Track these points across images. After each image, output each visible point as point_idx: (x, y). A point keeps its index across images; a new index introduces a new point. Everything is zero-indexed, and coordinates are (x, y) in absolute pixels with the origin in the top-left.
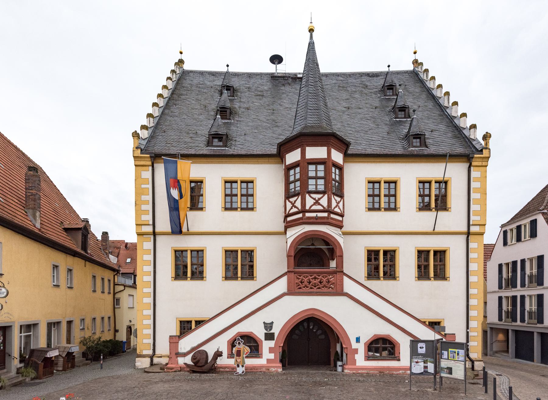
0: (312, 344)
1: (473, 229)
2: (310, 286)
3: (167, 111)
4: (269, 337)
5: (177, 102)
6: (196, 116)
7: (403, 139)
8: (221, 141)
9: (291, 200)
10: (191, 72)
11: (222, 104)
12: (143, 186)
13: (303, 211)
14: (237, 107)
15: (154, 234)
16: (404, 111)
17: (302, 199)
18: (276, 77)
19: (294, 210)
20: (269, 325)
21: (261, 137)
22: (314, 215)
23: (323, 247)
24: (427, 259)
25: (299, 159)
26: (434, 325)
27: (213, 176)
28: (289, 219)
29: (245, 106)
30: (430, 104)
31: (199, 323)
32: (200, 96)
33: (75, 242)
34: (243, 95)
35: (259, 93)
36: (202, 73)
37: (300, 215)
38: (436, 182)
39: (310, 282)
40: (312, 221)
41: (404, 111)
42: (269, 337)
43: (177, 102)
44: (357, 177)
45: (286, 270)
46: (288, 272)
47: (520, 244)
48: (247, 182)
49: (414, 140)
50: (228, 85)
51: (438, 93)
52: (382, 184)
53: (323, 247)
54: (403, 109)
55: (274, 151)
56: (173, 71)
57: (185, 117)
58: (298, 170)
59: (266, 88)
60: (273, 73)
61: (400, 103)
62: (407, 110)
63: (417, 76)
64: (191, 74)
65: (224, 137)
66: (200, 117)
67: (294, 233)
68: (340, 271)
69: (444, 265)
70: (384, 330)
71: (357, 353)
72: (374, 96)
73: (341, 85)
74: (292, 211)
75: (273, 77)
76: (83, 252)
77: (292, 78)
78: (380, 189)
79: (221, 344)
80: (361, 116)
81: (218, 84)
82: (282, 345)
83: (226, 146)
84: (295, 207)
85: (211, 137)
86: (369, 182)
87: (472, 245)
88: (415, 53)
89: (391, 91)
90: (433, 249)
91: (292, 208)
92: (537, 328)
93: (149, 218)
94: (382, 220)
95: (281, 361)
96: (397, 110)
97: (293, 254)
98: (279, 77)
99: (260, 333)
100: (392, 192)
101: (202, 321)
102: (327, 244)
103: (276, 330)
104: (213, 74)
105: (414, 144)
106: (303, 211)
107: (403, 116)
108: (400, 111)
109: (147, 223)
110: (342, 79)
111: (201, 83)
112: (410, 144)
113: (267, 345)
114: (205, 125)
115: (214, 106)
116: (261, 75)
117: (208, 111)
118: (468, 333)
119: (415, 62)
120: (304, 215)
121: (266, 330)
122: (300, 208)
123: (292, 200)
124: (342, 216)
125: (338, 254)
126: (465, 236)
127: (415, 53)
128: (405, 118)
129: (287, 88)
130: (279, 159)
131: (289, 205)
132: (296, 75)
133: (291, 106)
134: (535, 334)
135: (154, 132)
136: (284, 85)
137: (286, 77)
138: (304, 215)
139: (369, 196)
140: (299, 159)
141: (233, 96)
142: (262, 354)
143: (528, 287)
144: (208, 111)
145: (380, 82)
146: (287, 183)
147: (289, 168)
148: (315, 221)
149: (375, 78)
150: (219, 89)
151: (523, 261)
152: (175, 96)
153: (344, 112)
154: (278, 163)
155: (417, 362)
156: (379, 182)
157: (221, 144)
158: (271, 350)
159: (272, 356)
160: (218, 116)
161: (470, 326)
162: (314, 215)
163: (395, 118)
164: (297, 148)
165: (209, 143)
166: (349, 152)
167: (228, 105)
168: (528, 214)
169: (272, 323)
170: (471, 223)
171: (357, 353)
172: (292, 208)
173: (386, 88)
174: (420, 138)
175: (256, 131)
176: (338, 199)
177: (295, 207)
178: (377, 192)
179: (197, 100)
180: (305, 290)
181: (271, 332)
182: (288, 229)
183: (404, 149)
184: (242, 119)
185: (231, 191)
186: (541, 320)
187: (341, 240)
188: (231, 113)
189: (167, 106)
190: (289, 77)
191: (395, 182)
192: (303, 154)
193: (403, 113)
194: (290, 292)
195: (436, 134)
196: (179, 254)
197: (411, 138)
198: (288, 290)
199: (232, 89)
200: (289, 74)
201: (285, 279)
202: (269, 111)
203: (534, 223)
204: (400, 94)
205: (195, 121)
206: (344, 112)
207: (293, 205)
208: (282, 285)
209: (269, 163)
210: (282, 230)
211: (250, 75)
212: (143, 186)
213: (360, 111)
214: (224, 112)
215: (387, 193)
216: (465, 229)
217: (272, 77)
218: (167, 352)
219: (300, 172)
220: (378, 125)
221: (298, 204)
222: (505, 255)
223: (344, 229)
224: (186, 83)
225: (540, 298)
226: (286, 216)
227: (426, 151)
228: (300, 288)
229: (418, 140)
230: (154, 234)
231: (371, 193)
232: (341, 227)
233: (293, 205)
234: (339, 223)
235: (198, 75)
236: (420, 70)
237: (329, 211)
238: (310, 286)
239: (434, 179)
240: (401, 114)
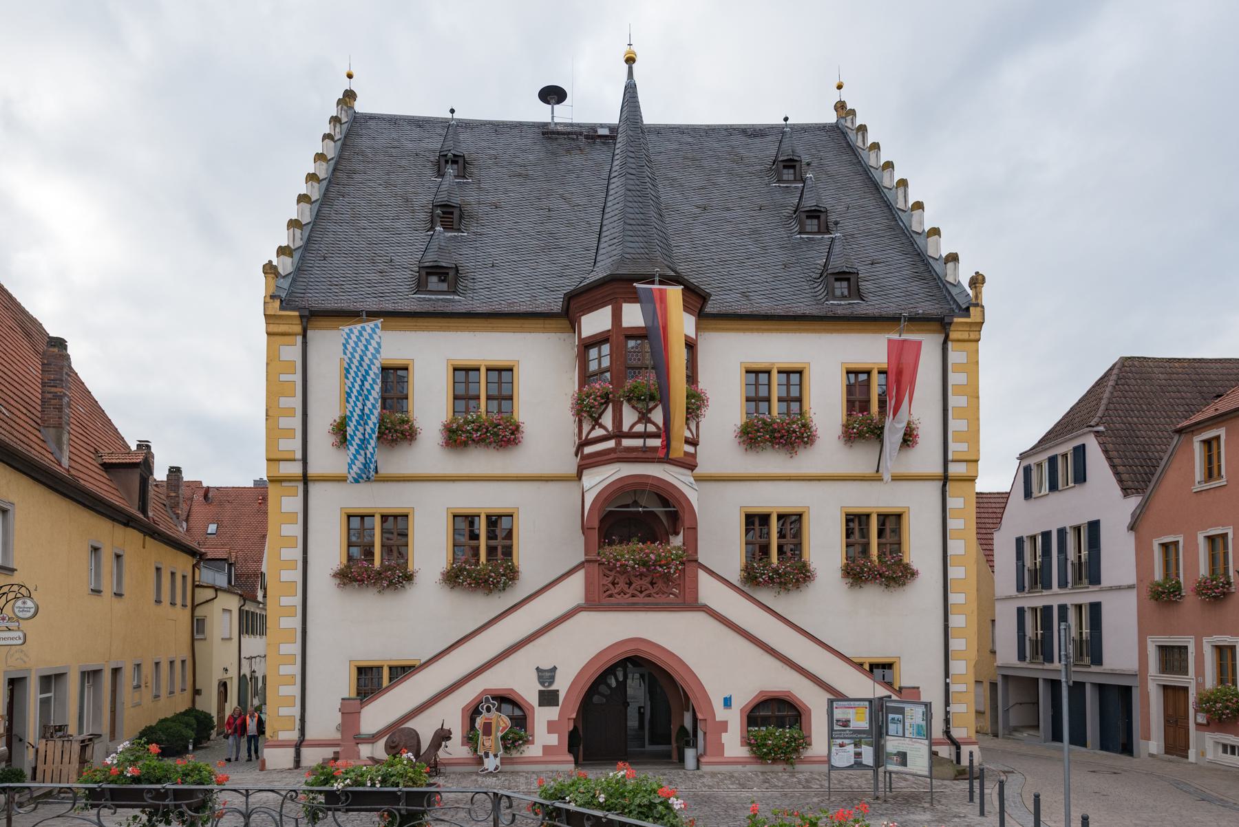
0: (635, 712)
1: (955, 469)
2: (631, 591)
3: (326, 210)
4: (548, 698)
5: (346, 190)
6: (388, 223)
7: (814, 280)
8: (443, 281)
10: (372, 117)
11: (443, 197)
13: (618, 435)
14: (470, 199)
15: (305, 479)
16: (818, 217)
17: (614, 410)
18: (553, 133)
19: (598, 432)
20: (548, 674)
21: (526, 271)
22: (638, 442)
23: (659, 510)
24: (865, 534)
25: (609, 327)
26: (880, 669)
27: (431, 359)
28: (588, 450)
29: (491, 198)
30: (870, 203)
31: (401, 672)
32: (393, 176)
33: (124, 493)
34: (483, 173)
35: (518, 170)
36: (394, 121)
37: (611, 444)
38: (880, 372)
39: (630, 584)
40: (634, 455)
41: (818, 217)
42: (548, 698)
43: (346, 190)
44: (726, 364)
45: (581, 558)
46: (587, 561)
47: (1055, 496)
48: (500, 370)
49: (837, 284)
50: (453, 151)
51: (887, 181)
52: (775, 374)
53: (659, 510)
54: (815, 214)
55: (557, 307)
56: (335, 120)
57: (366, 224)
58: (606, 349)
59: (531, 157)
60: (546, 124)
61: (809, 203)
62: (823, 216)
63: (842, 138)
64: (372, 123)
65: (452, 273)
66: (397, 225)
67: (598, 480)
68: (690, 560)
69: (900, 544)
70: (782, 681)
71: (726, 731)
72: (756, 181)
73: (689, 155)
74: (591, 436)
75: (548, 133)
76: (141, 516)
77: (587, 137)
78: (769, 385)
79: (451, 715)
80: (729, 228)
81: (430, 146)
82: (574, 716)
83: (455, 293)
84: (601, 426)
85: (423, 273)
86: (747, 372)
87: (952, 503)
88: (840, 87)
89: (792, 171)
90: (875, 510)
92: (1090, 675)
93: (295, 445)
95: (572, 748)
96: (804, 216)
97: (596, 524)
98: (559, 133)
99: (529, 692)
100: (794, 392)
101: (410, 667)
102: (665, 502)
103: (562, 685)
104: (420, 123)
105: (838, 292)
106: (618, 435)
107: (815, 229)
108: (808, 217)
109: (291, 457)
110: (690, 140)
111: (396, 144)
112: (831, 294)
113: (543, 717)
114: (411, 244)
115: (424, 199)
116: (519, 126)
117: (413, 211)
118: (947, 685)
119: (840, 106)
120: (618, 444)
121: (542, 683)
122: (610, 429)
124: (694, 443)
125: (687, 525)
126: (940, 484)
127: (840, 87)
128: (819, 232)
129: (577, 159)
130: (565, 323)
132: (593, 128)
133: (584, 200)
134: (1088, 687)
135: (302, 258)
136: (568, 151)
137: (575, 133)
138: (618, 444)
139: (748, 400)
140: (609, 327)
141: (464, 177)
142: (532, 736)
143: (1073, 588)
144: (413, 211)
145: (768, 150)
146: (585, 377)
147: (588, 345)
148: (640, 455)
149: (757, 140)
150: (432, 159)
151: (1062, 532)
152: (338, 174)
153: (695, 218)
154: (562, 331)
155: (841, 746)
156: (769, 372)
157: (444, 286)
158: (552, 727)
159: (553, 740)
160: (439, 229)
161: (951, 672)
162: (638, 442)
163: (800, 233)
164: (603, 305)
165: (420, 286)
166: (710, 308)
167: (456, 200)
168: (1071, 431)
169: (555, 668)
170: (950, 457)
171: (726, 731)
172: (593, 428)
173: (781, 165)
174: (848, 280)
175: (515, 258)
177: (601, 426)
178: (763, 392)
179: (387, 184)
180: (619, 599)
181: (553, 688)
182: (585, 472)
183: (818, 302)
184: (485, 230)
185: (467, 389)
186: (1097, 659)
187: (692, 496)
188: (461, 217)
189: (326, 198)
190: (581, 134)
191: (800, 372)
193: (815, 221)
194: (593, 603)
195: (880, 269)
196: (356, 521)
197: (832, 279)
198: (587, 599)
199: (461, 161)
200: (579, 125)
201: (580, 576)
202: (541, 212)
203: (1080, 452)
204: (808, 182)
205: (385, 234)
206: (695, 218)
208: (574, 590)
210: (573, 470)
211: (497, 128)
213: (727, 214)
214: (448, 215)
215: (784, 394)
216: (939, 470)
217: (543, 134)
218: (333, 734)
219: (611, 355)
220: (764, 248)
222: (1024, 519)
223: (697, 471)
224: (364, 143)
225: (1096, 608)
226: (582, 445)
227: (862, 308)
228: (611, 596)
229: (845, 284)
230: (305, 479)
231: (753, 395)
232: (692, 467)
234: (689, 460)
235: (387, 126)
236: (849, 124)
238: (631, 591)
239: (876, 367)
240: (812, 225)
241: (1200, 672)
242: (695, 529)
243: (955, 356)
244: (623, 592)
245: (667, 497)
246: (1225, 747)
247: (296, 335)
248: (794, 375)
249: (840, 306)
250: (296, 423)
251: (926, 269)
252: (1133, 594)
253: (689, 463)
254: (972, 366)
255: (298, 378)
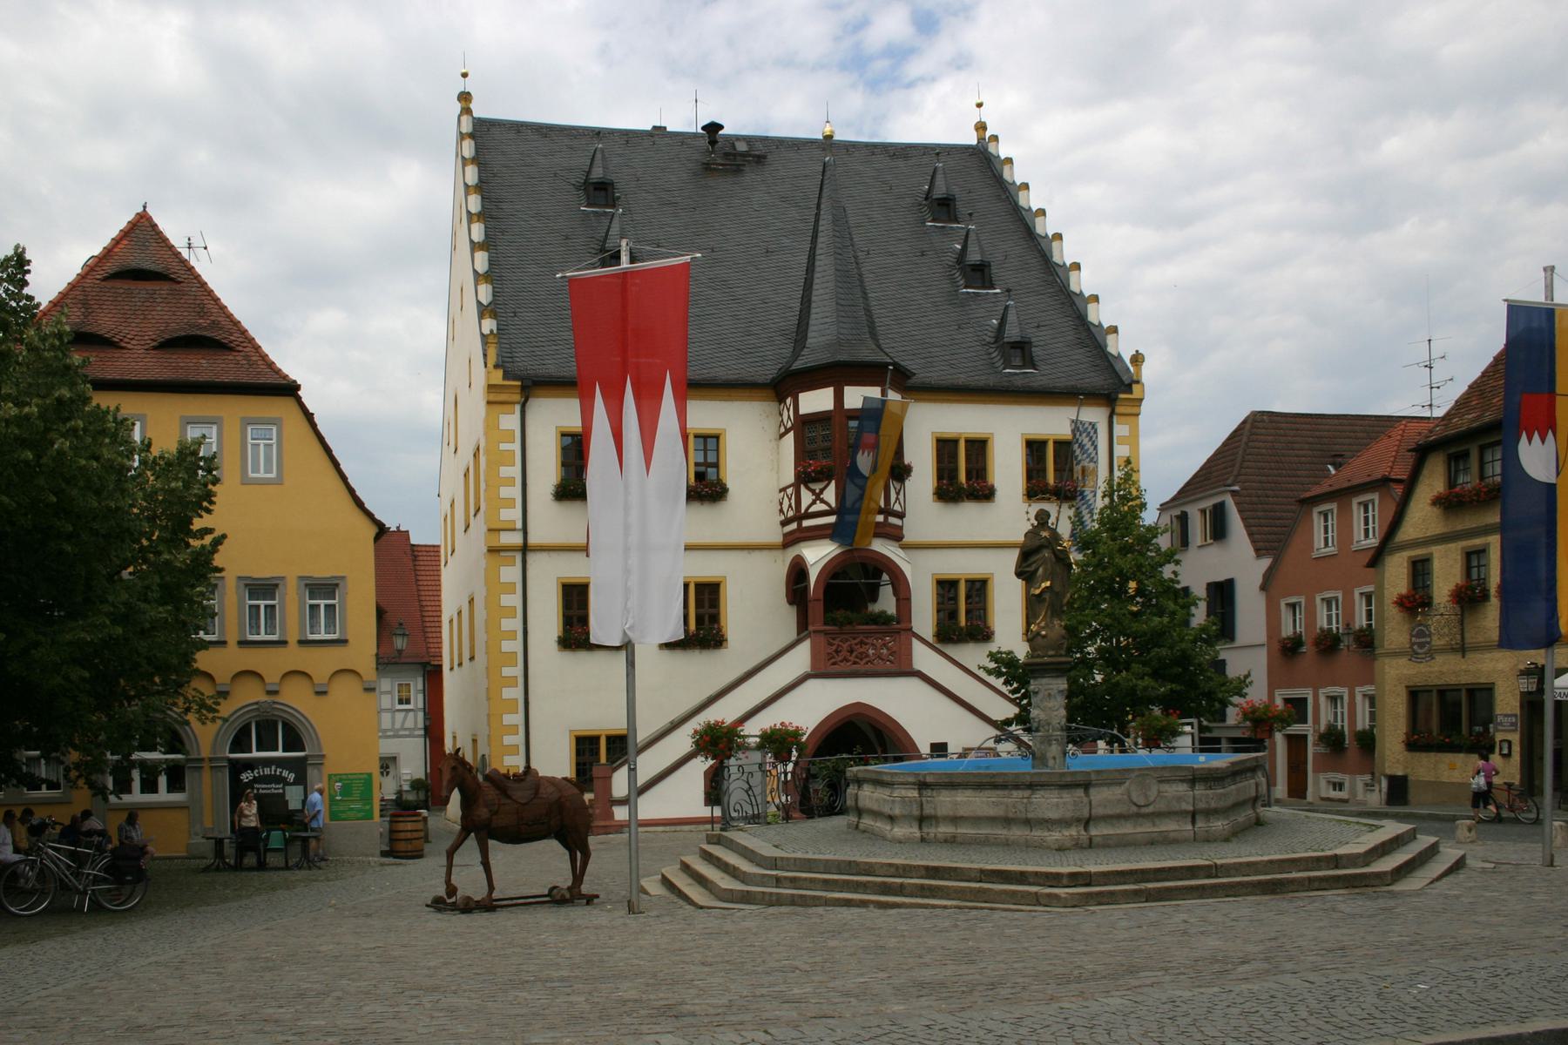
9: (812, 486)
12: (503, 446)
19: (819, 507)
84: (823, 501)
91: (814, 503)
94: (967, 520)
123: (817, 487)
124: (901, 516)
131: (806, 497)
172: (814, 503)
176: (898, 486)
177: (823, 501)
192: (839, 398)
194: (822, 669)
207: (818, 497)
209: (751, 399)
212: (503, 446)
221: (830, 495)
233: (818, 497)
237: (888, 512)
241: (1317, 720)
242: (909, 599)
243: (1120, 429)
244: (846, 660)
245: (878, 568)
246: (1334, 785)
247: (513, 403)
248: (978, 447)
249: (1013, 373)
250: (516, 492)
251: (1092, 339)
252: (1263, 653)
253: (896, 535)
254: (1133, 440)
255: (517, 447)
